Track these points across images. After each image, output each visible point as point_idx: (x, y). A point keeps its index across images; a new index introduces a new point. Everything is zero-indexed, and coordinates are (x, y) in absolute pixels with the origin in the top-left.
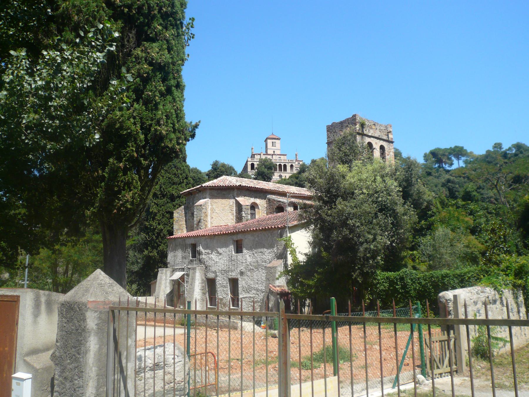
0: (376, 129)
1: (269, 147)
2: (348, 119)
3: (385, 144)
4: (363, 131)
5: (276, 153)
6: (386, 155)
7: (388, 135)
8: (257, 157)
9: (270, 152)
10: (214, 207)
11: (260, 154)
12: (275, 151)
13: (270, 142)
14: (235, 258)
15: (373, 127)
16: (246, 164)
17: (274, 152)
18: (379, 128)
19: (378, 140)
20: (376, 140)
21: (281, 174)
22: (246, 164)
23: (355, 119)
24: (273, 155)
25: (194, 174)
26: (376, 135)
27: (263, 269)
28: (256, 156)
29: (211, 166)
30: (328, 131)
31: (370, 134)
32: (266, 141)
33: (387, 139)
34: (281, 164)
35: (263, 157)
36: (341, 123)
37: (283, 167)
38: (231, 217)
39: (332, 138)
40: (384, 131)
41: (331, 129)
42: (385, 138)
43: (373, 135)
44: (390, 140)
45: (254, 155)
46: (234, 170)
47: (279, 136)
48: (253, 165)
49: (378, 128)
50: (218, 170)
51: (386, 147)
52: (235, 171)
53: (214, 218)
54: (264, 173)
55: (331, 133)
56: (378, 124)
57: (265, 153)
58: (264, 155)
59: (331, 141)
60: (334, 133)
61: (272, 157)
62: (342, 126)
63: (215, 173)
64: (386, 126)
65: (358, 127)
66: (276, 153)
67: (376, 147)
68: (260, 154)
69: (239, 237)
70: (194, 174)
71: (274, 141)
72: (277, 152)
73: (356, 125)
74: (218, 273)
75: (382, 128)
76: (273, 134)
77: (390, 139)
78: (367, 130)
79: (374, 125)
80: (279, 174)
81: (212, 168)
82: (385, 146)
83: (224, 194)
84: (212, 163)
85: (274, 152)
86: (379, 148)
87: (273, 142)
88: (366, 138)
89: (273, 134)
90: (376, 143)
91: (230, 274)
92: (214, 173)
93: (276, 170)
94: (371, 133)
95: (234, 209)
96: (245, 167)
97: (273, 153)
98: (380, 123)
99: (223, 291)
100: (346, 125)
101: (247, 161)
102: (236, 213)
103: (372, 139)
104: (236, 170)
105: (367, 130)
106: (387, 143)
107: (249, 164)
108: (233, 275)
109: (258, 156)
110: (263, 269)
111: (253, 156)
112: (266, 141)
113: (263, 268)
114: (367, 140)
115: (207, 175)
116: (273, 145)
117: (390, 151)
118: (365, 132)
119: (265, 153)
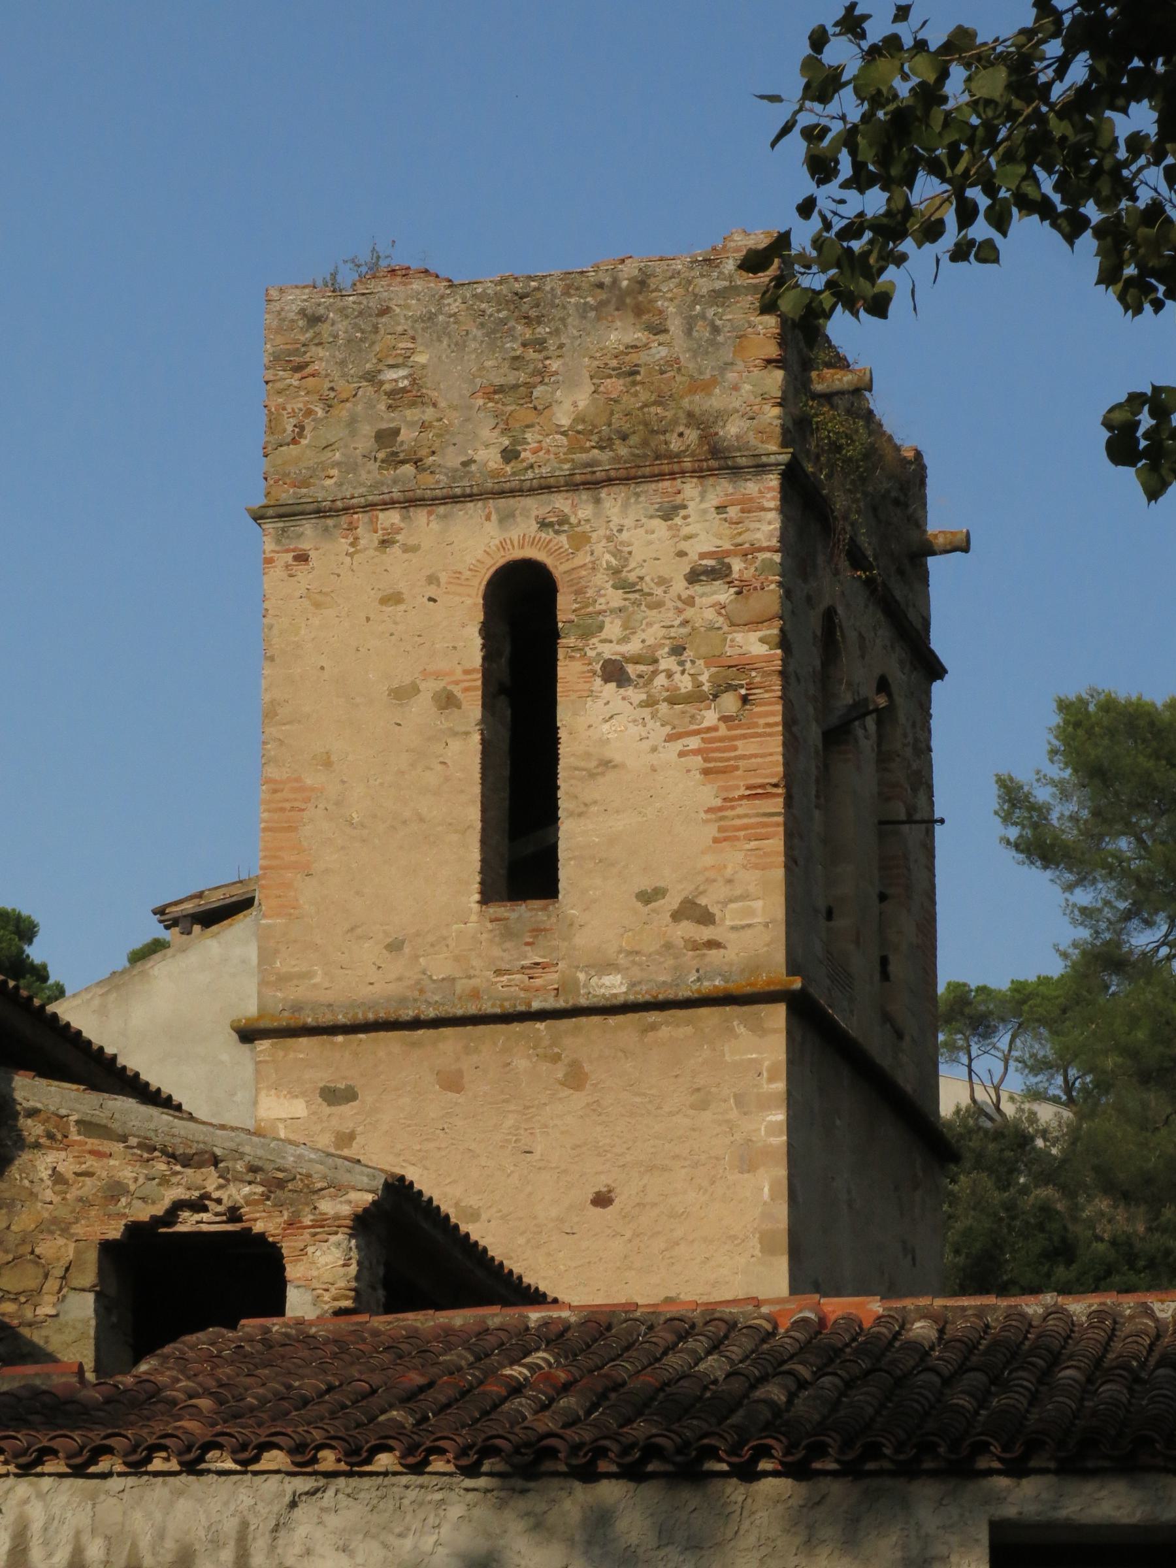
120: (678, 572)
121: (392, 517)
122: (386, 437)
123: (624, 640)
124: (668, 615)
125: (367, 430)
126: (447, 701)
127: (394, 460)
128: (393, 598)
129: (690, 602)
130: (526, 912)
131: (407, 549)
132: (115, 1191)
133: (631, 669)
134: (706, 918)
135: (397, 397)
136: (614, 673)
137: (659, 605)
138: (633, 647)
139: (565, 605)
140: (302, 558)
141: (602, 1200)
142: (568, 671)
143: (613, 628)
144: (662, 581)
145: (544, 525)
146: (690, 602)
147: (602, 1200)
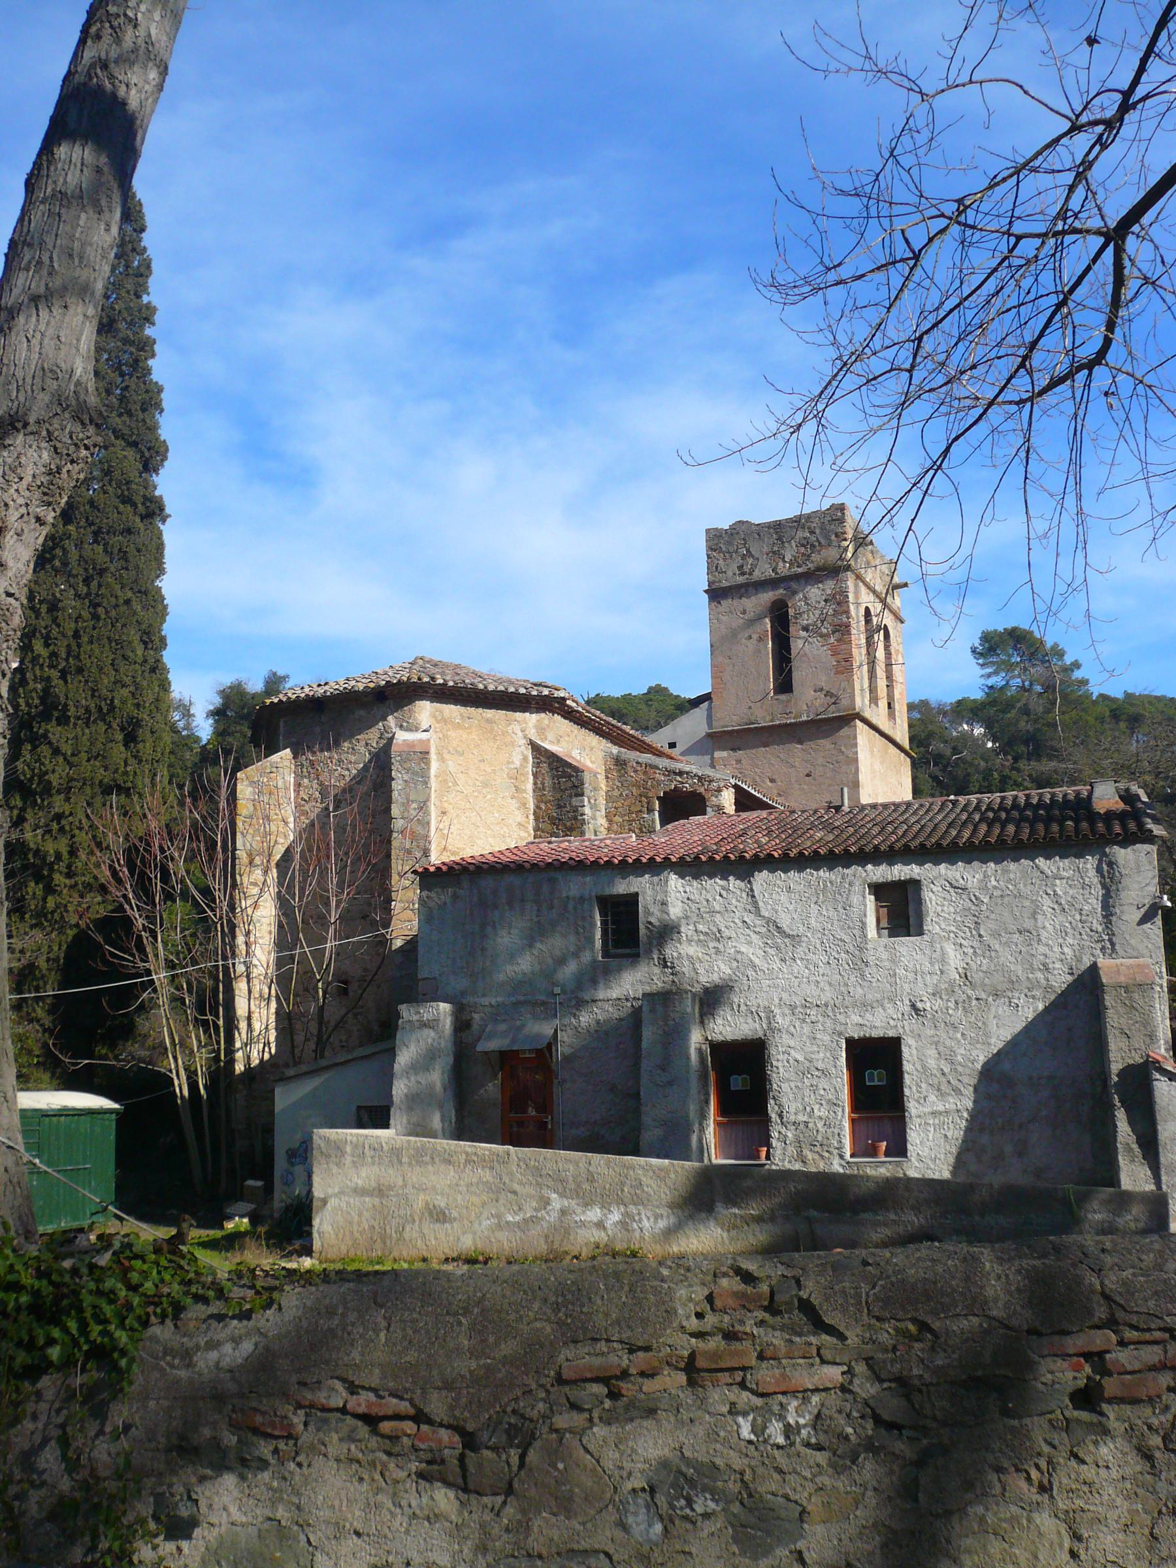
10: (451, 766)
14: (885, 956)
23: (842, 521)
27: (1033, 997)
30: (710, 548)
38: (519, 817)
39: (731, 577)
53: (452, 813)
59: (725, 584)
69: (900, 872)
74: (779, 1019)
83: (488, 721)
91: (856, 1019)
95: (529, 786)
99: (814, 1088)
102: (540, 798)
108: (878, 1024)
110: (1033, 997)
113: (1037, 993)
122: (740, 567)
125: (734, 567)
130: (783, 697)
132: (659, 782)
135: (743, 557)
136: (806, 629)
139: (791, 612)
141: (808, 775)
147: (808, 775)
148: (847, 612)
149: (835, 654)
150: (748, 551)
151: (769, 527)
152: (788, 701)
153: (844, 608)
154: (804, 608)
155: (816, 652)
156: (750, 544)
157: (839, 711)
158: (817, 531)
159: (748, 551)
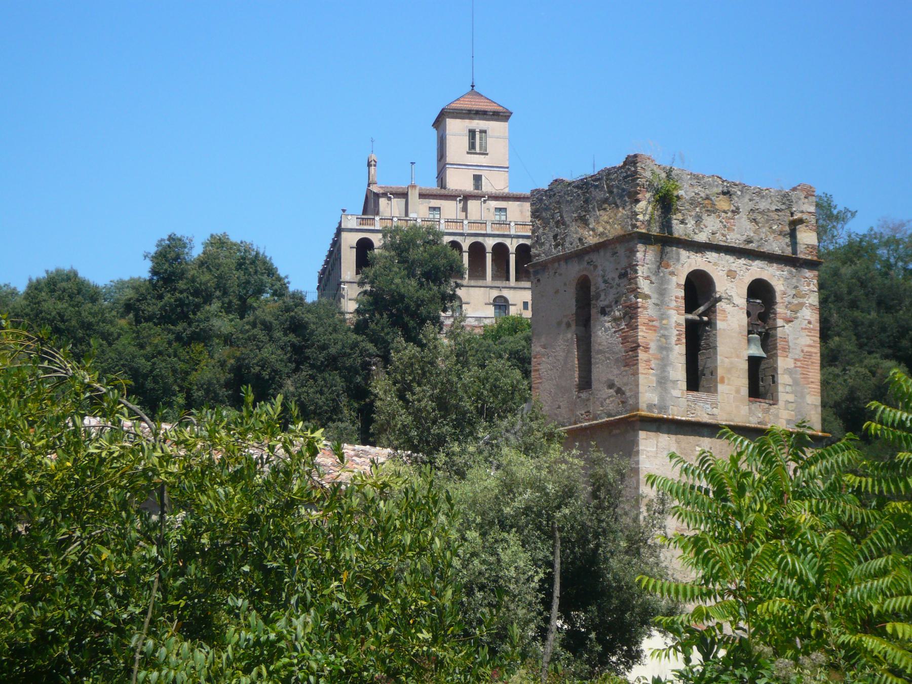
0: (736, 211)
1: (450, 157)
2: (608, 172)
3: (773, 274)
4: (666, 225)
5: (487, 187)
6: (780, 322)
7: (793, 235)
8: (391, 209)
9: (458, 181)
11: (404, 195)
12: (484, 173)
13: (456, 128)
15: (723, 204)
16: (336, 244)
17: (477, 179)
18: (751, 205)
19: (742, 261)
20: (730, 258)
21: (506, 293)
22: (336, 244)
23: (634, 175)
24: (466, 197)
25: (60, 306)
26: (735, 239)
28: (383, 201)
29: (149, 264)
31: (702, 237)
32: (439, 123)
33: (788, 251)
34: (507, 242)
35: (420, 212)
36: (585, 185)
37: (512, 258)
40: (774, 216)
41: (547, 209)
42: (778, 246)
43: (719, 240)
44: (803, 254)
45: (377, 196)
46: (271, 271)
47: (504, 101)
48: (364, 246)
49: (745, 205)
50: (181, 285)
51: (779, 286)
52: (279, 279)
54: (402, 297)
55: (546, 223)
56: (744, 188)
57: (432, 185)
58: (422, 196)
60: (558, 223)
61: (465, 209)
62: (586, 201)
63: (168, 297)
64: (786, 196)
65: (645, 207)
66: (486, 187)
67: (732, 293)
68: (404, 195)
70: (60, 306)
71: (478, 124)
72: (494, 183)
73: (637, 201)
75: (763, 205)
76: (473, 91)
77: (801, 248)
78: (691, 223)
79: (724, 193)
80: (495, 293)
81: (154, 272)
82: (774, 282)
84: (153, 250)
85: (477, 179)
86: (744, 292)
87: (472, 133)
88: (684, 253)
89: (473, 91)
90: (731, 274)
92: (160, 297)
93: (523, 251)
94: (709, 230)
96: (331, 253)
97: (468, 186)
98: (754, 183)
100: (600, 195)
101: (339, 231)
103: (712, 256)
104: (282, 273)
105: (691, 223)
106: (786, 270)
107: (350, 240)
109: (395, 201)
111: (371, 204)
112: (439, 123)
114: (690, 262)
115: (129, 307)
116: (472, 146)
117: (802, 305)
118: (679, 230)
119: (432, 185)
120: (615, 275)
121: (556, 265)
122: (555, 237)
123: (605, 300)
124: (613, 291)
125: (551, 235)
126: (568, 325)
127: (557, 246)
128: (557, 292)
129: (619, 285)
130: (584, 395)
131: (560, 275)
133: (607, 310)
134: (623, 393)
137: (611, 287)
138: (606, 303)
140: (539, 280)
142: (593, 311)
143: (602, 297)
144: (613, 279)
145: (588, 263)
146: (619, 285)
148: (635, 291)
149: (625, 340)
150: (562, 216)
151: (577, 187)
152: (588, 400)
153: (633, 286)
154: (603, 286)
155: (611, 340)
156: (565, 208)
157: (626, 411)
158: (615, 190)
159: (562, 216)
